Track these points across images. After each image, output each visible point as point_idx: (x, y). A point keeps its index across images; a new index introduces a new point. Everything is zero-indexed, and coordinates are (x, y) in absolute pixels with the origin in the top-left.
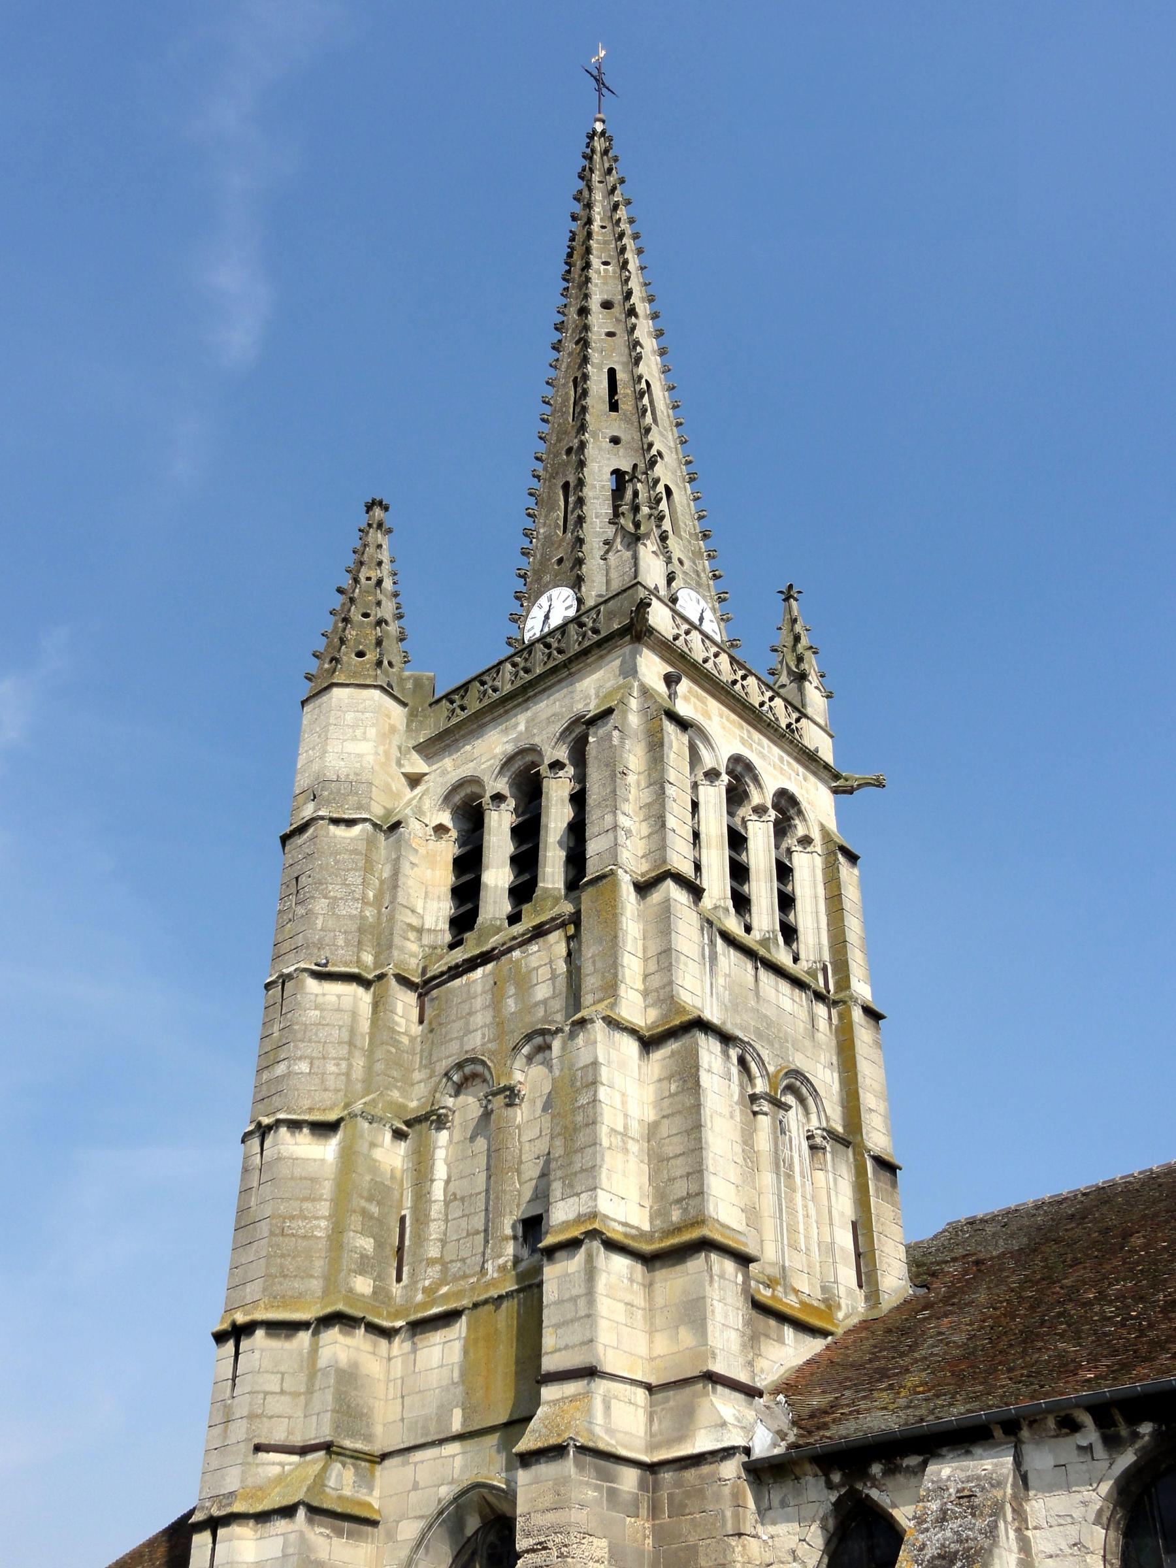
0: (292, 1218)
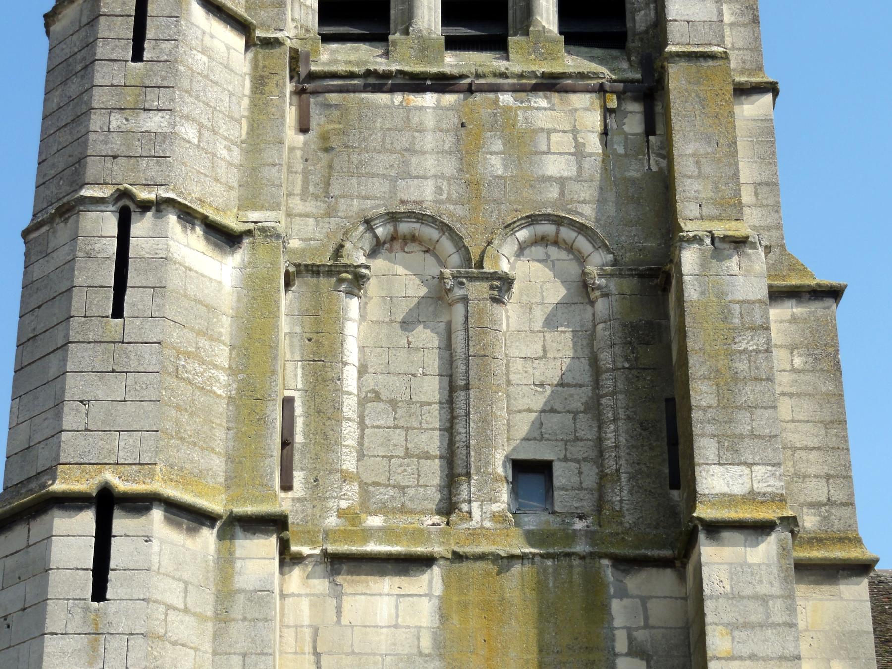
0: (188, 355)
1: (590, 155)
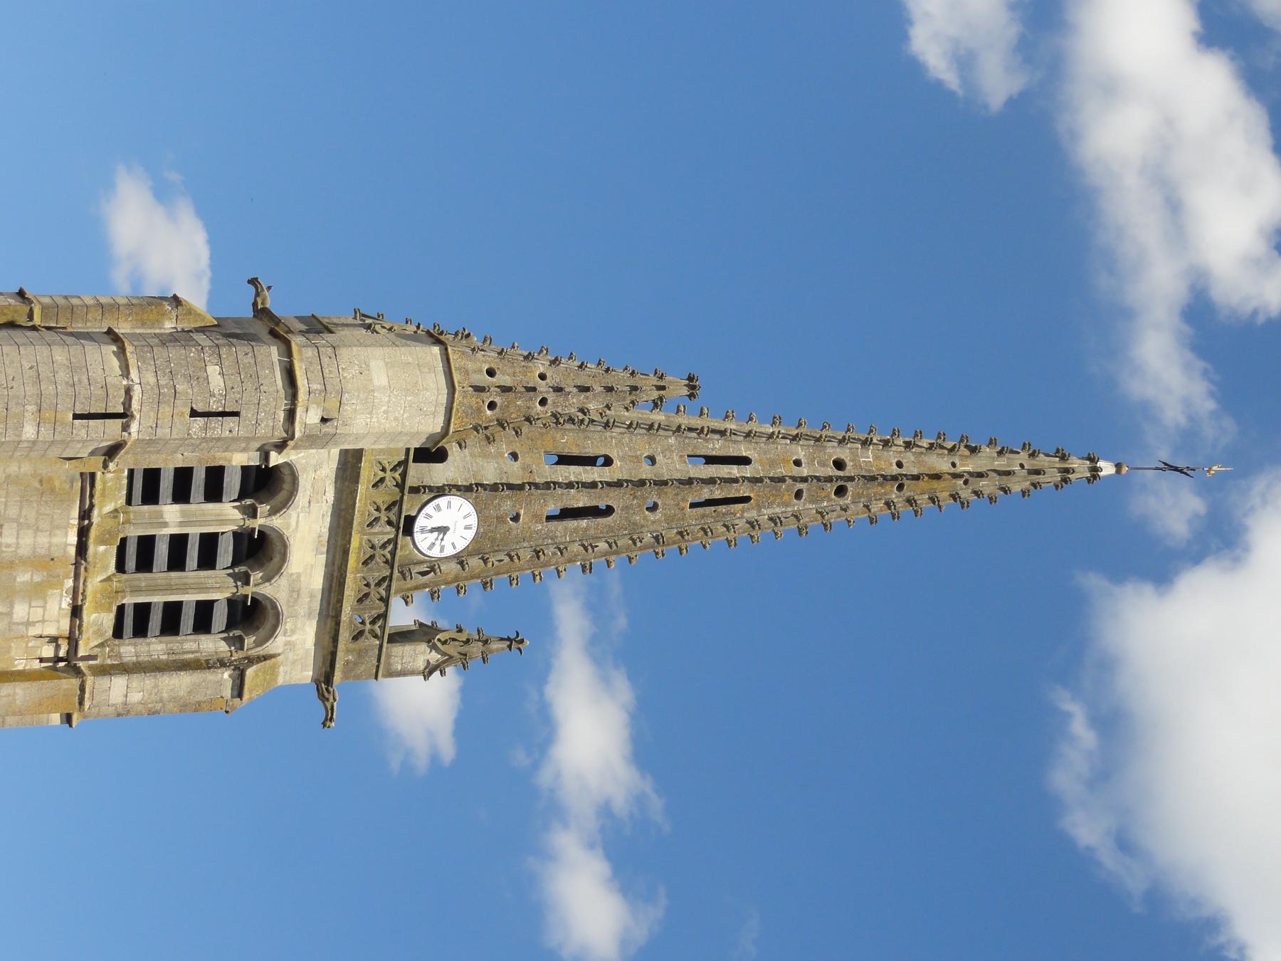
1: (27, 630)
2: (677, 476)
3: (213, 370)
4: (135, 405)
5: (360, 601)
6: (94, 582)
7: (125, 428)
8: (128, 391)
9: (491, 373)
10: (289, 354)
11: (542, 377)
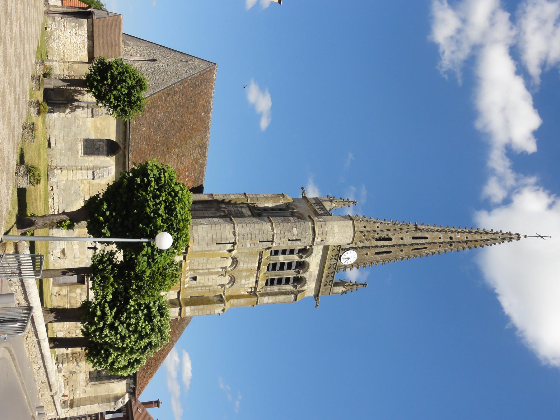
2: (409, 243)
3: (294, 229)
4: (275, 239)
5: (327, 277)
6: (261, 275)
7: (272, 244)
8: (273, 235)
9: (365, 227)
10: (314, 224)
11: (378, 227)
